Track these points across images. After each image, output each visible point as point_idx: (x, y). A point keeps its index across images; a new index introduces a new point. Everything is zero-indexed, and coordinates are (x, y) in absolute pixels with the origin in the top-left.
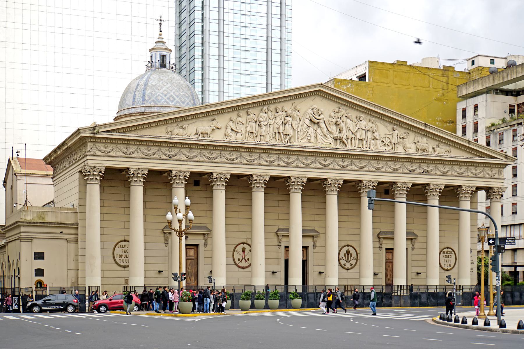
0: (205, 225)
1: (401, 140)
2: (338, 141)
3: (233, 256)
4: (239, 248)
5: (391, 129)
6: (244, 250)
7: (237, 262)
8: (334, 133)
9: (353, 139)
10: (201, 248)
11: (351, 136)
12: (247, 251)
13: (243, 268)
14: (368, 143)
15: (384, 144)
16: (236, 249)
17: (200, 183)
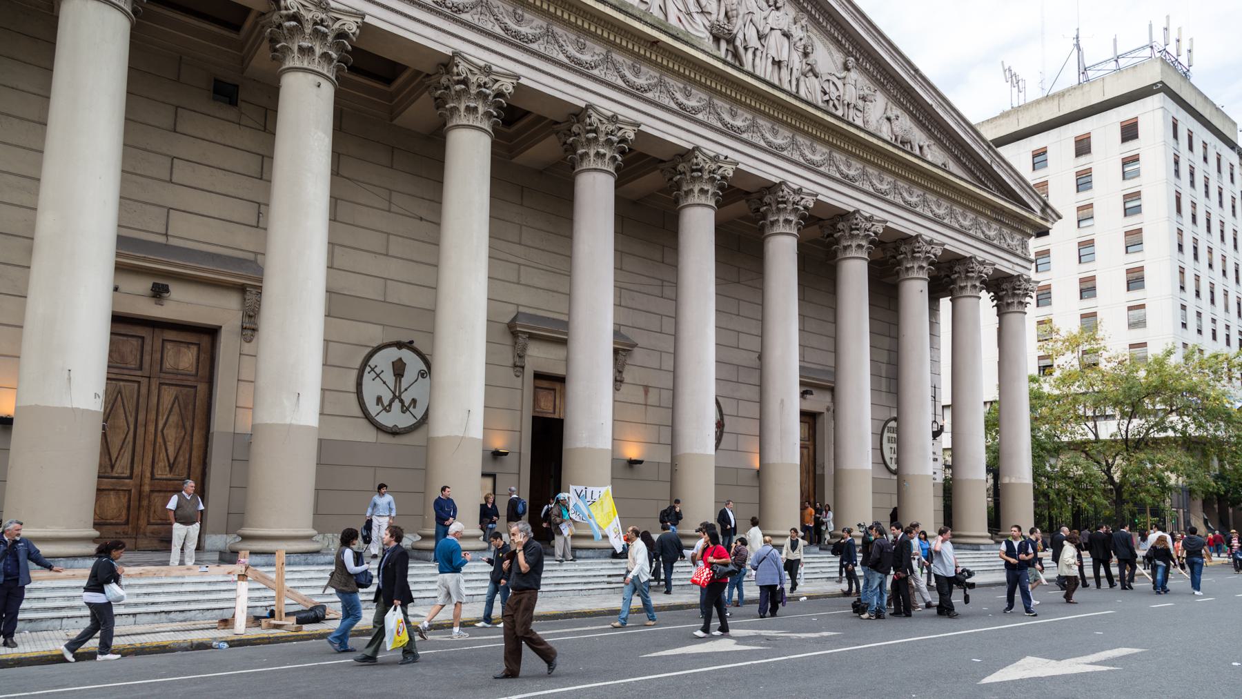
0: (251, 257)
1: (860, 103)
2: (723, 45)
3: (359, 384)
4: (383, 361)
5: (840, 66)
6: (399, 369)
7: (373, 409)
8: (714, 17)
9: (758, 53)
10: (227, 344)
11: (754, 42)
12: (410, 374)
13: (394, 432)
14: (794, 83)
15: (827, 97)
16: (372, 363)
17: (242, 95)
